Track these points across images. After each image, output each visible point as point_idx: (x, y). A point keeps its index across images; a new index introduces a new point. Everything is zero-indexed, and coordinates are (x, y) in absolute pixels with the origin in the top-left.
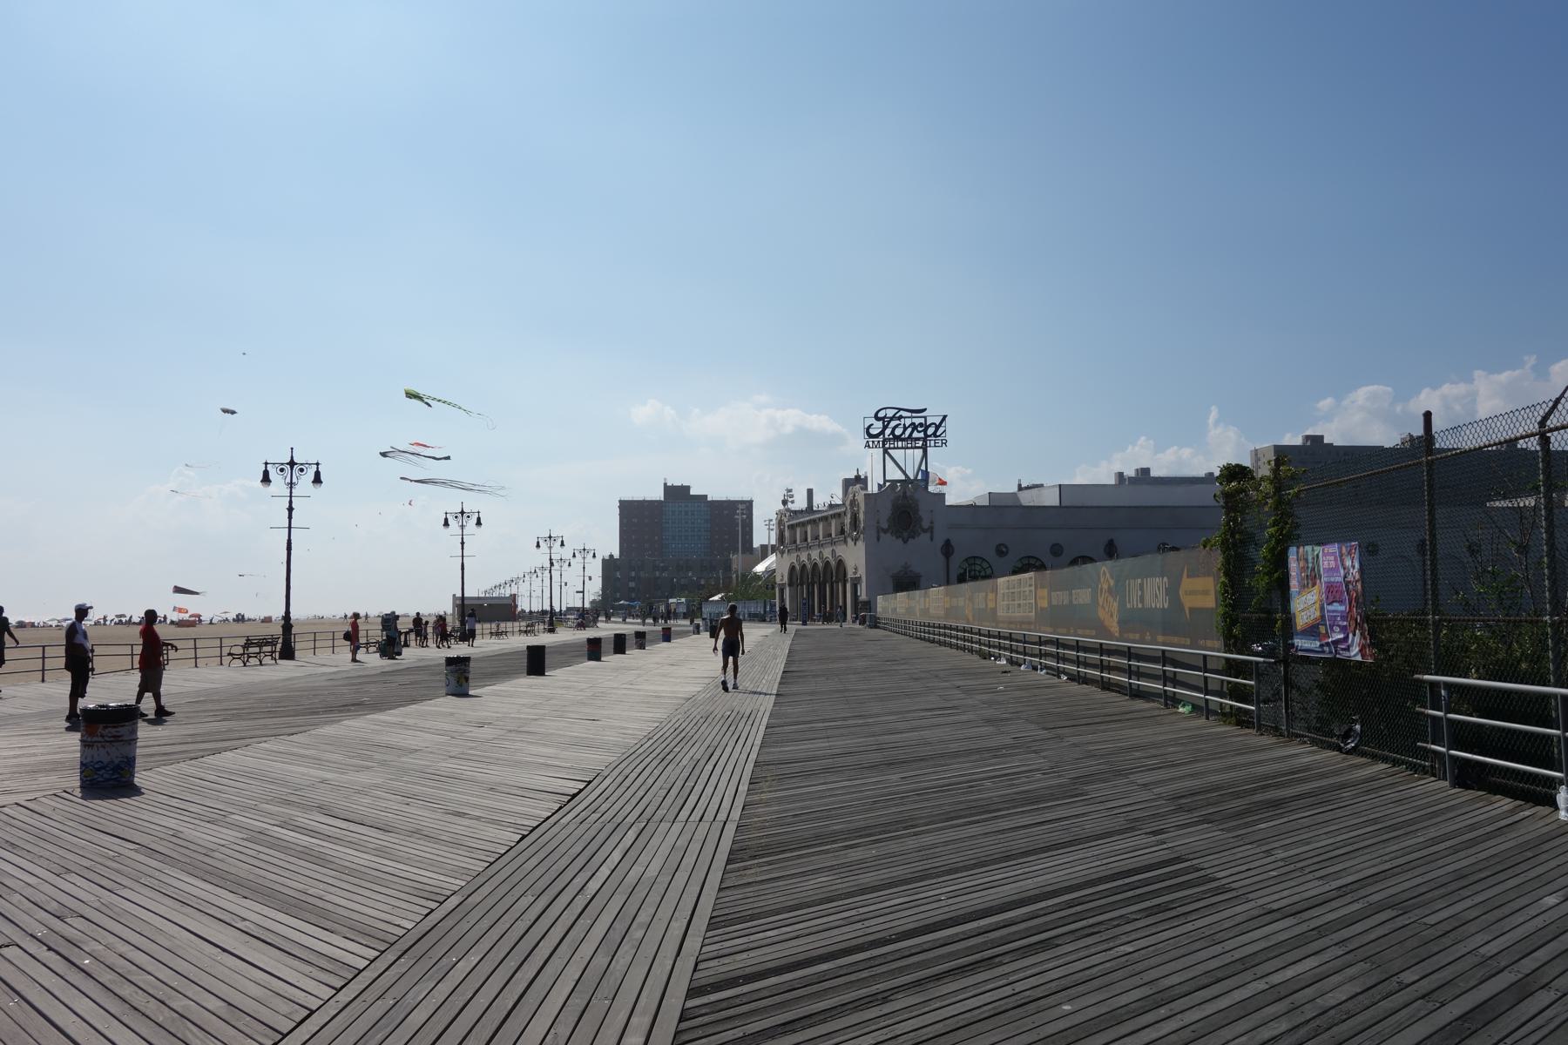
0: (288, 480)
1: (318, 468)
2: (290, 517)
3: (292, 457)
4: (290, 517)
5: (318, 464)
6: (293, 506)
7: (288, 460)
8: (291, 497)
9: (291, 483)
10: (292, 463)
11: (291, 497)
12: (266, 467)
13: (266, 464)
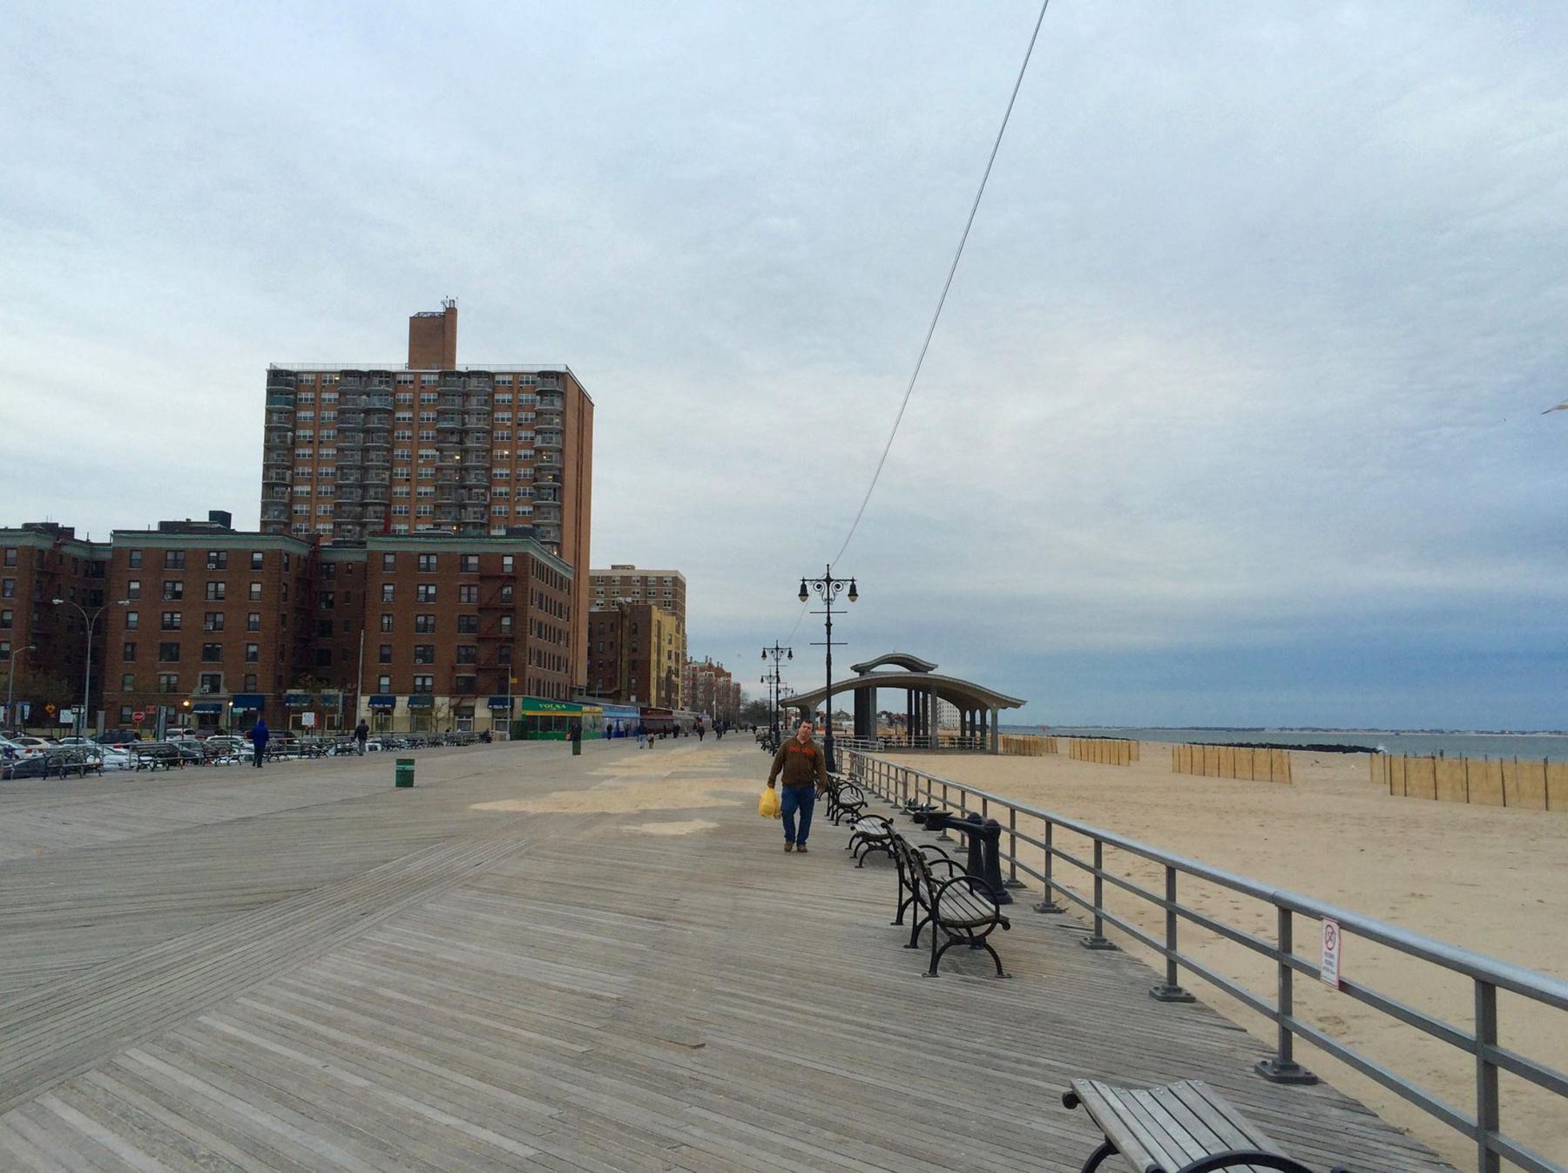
0: (825, 596)
2: (829, 633)
3: (828, 574)
4: (829, 633)
5: (853, 580)
8: (829, 612)
9: (828, 599)
11: (829, 612)
13: (804, 580)
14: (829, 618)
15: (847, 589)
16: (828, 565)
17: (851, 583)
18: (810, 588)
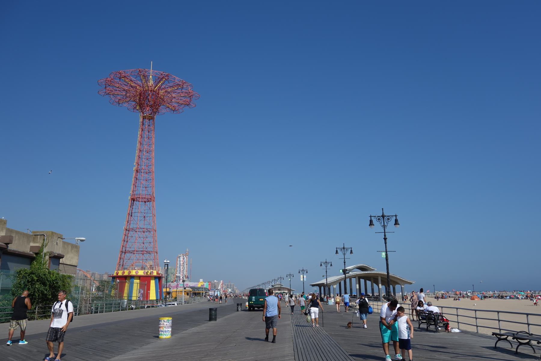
0: (382, 224)
1: (396, 218)
2: (386, 243)
4: (386, 243)
6: (387, 237)
7: (381, 214)
10: (383, 216)
12: (371, 218)
14: (385, 235)
15: (393, 221)
16: (383, 209)
17: (394, 218)
18: (374, 221)
